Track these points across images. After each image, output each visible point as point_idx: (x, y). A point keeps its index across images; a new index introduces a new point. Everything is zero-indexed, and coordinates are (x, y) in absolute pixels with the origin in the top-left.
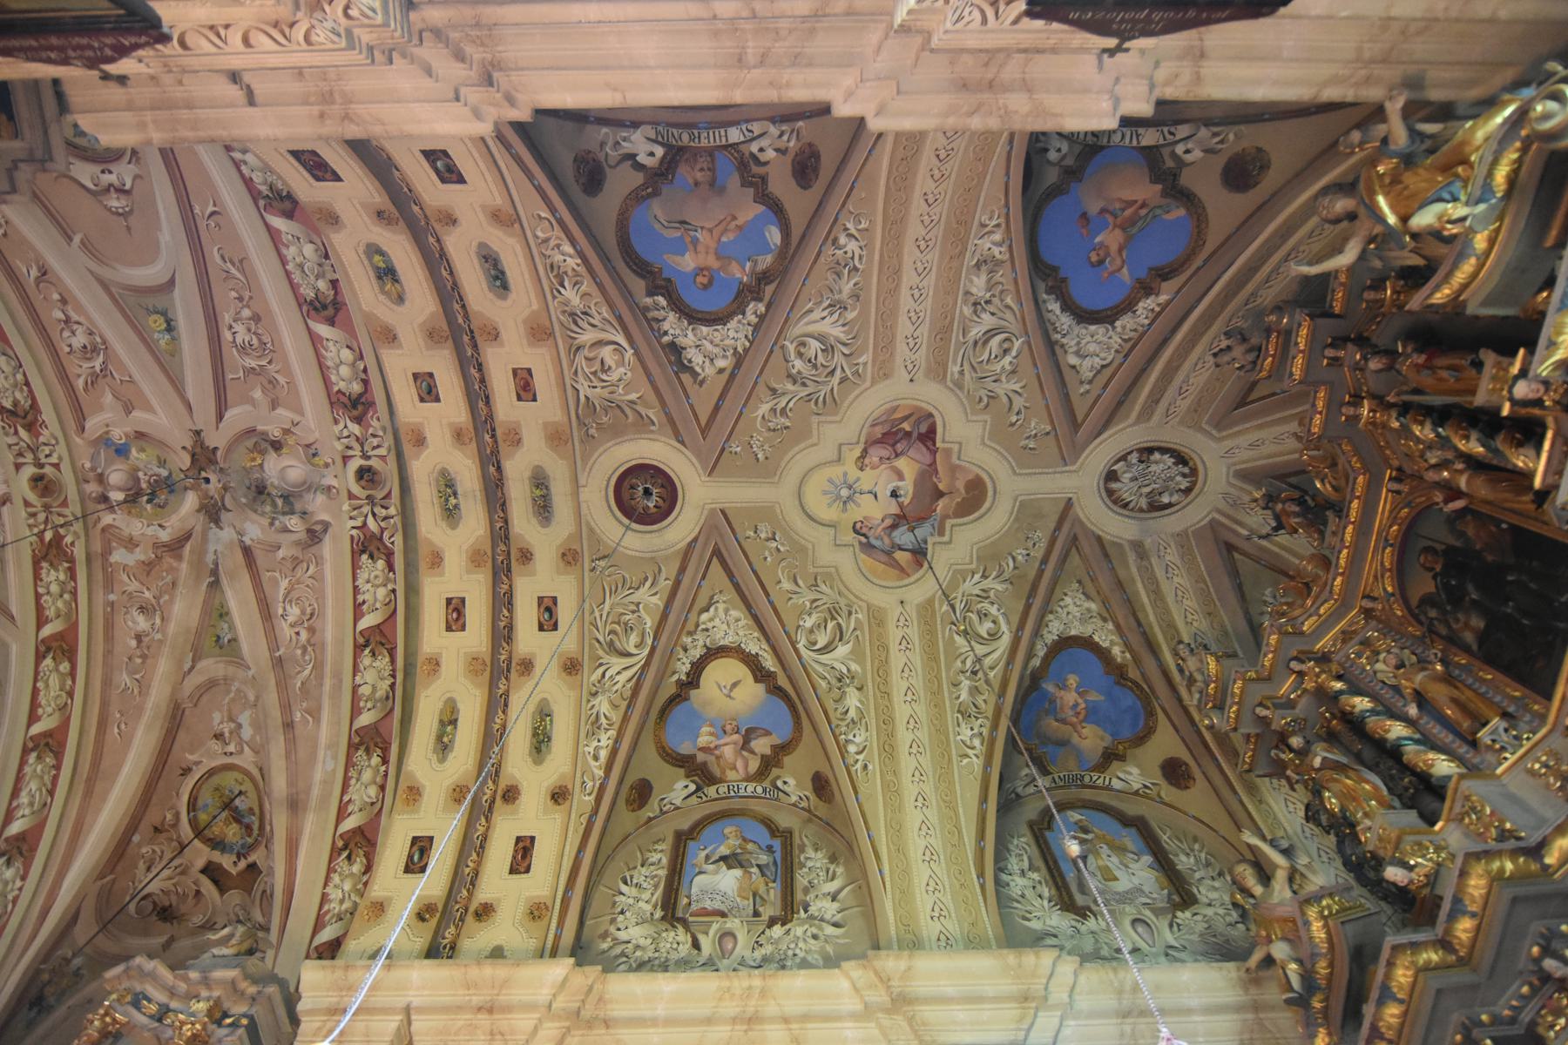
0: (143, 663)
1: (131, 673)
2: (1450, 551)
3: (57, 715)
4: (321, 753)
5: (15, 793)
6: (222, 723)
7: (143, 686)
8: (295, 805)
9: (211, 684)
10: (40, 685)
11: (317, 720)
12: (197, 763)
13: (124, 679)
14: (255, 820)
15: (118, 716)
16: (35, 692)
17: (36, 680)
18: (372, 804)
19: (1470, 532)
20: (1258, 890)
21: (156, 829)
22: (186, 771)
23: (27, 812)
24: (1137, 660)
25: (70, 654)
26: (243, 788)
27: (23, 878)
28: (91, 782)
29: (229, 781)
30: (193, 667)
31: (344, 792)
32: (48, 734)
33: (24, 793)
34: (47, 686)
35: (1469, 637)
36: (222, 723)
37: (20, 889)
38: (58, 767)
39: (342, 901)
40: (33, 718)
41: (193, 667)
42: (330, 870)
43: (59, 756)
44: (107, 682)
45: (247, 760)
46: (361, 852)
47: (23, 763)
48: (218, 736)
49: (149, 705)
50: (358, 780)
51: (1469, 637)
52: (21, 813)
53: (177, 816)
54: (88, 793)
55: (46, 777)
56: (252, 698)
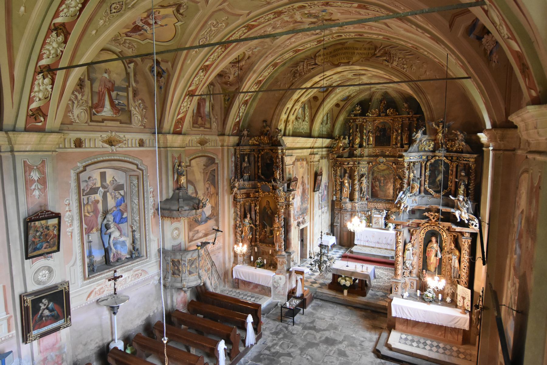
2: (385, 128)
8: (254, 72)
16: (235, 33)
20: (341, 139)
23: (211, 60)
24: (352, 98)
27: (204, 76)
38: (223, 52)
51: (377, 134)
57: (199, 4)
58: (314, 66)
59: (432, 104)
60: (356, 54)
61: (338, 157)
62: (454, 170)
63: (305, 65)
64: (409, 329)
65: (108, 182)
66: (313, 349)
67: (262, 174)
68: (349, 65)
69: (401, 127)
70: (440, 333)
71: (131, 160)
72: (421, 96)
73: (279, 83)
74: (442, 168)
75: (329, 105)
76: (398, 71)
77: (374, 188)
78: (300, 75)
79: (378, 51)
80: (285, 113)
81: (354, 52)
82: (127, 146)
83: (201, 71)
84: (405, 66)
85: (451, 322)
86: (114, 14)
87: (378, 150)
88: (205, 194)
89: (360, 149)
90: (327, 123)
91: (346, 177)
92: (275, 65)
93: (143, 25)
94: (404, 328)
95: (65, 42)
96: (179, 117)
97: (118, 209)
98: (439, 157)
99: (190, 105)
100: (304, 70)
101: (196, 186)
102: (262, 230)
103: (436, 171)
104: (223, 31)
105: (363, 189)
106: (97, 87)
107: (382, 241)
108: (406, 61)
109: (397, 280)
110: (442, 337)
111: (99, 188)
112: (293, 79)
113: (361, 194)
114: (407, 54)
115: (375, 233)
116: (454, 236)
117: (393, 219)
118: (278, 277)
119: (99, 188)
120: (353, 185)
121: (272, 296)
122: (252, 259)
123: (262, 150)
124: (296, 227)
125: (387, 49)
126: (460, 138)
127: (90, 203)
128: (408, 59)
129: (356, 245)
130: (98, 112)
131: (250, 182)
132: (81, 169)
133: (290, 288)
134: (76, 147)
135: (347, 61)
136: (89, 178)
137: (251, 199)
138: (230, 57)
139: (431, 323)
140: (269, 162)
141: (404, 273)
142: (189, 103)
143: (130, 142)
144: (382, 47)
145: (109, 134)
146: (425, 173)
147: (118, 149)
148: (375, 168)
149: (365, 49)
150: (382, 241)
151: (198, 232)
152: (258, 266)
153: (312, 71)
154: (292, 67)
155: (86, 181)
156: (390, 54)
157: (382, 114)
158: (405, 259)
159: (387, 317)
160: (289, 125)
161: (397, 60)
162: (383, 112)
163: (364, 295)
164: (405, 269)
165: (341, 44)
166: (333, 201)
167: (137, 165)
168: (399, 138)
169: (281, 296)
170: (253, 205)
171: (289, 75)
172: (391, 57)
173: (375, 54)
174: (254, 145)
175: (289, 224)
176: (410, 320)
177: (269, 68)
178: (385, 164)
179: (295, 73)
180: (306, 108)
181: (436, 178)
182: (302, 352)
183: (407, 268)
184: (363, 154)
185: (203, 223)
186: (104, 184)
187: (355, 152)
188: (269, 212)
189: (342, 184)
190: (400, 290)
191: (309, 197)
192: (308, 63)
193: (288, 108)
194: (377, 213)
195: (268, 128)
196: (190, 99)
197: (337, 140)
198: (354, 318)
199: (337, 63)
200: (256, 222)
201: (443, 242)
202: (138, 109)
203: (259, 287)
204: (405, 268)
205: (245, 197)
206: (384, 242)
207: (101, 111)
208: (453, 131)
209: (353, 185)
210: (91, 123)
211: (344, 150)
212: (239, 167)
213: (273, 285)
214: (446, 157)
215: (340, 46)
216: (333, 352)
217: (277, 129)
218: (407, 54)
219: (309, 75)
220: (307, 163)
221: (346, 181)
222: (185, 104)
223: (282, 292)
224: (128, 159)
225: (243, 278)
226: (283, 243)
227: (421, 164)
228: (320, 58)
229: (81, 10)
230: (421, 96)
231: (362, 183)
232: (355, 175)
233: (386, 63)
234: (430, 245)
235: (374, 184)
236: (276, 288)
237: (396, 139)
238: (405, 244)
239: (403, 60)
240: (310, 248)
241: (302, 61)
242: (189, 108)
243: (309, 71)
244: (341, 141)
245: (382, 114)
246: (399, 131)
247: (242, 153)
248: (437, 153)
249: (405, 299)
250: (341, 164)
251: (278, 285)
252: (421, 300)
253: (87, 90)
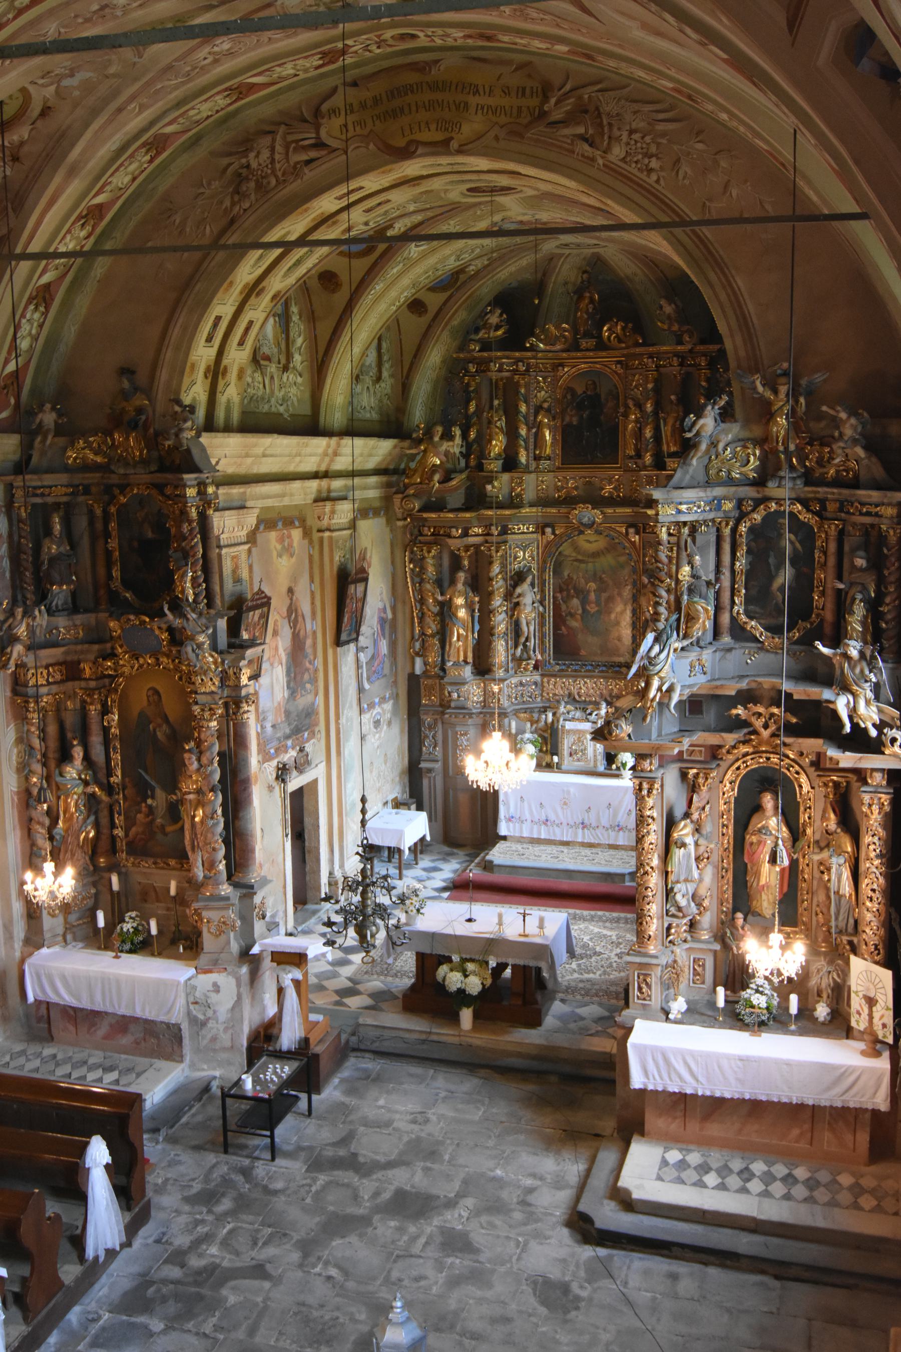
2: (598, 396)
8: (72, 172)
11: (140, 113)
19: (610, 404)
20: (436, 439)
31: (112, 175)
35: (567, 419)
51: (567, 419)
56: (112, 70)
58: (313, 154)
59: (751, 308)
60: (472, 110)
61: (424, 509)
62: (832, 547)
63: (279, 148)
64: (693, 1126)
66: (347, 1240)
67: (127, 583)
68: (449, 153)
69: (653, 389)
70: (796, 1132)
72: (712, 276)
73: (178, 219)
74: (788, 541)
75: (382, 307)
76: (627, 179)
77: (564, 622)
78: (259, 186)
79: (553, 101)
80: (209, 339)
81: (466, 104)
84: (654, 164)
85: (829, 1089)
87: (573, 481)
89: (506, 477)
90: (379, 379)
91: (460, 586)
92: (157, 145)
94: (674, 1126)
98: (779, 501)
100: (274, 172)
102: (139, 804)
103: (772, 553)
105: (525, 629)
107: (598, 820)
108: (659, 145)
109: (646, 955)
110: (803, 1145)
112: (233, 204)
113: (516, 647)
114: (661, 116)
115: (572, 790)
116: (836, 785)
117: (624, 735)
118: (205, 981)
120: (484, 615)
121: (187, 1059)
122: (101, 923)
123: (123, 488)
124: (275, 784)
125: (586, 93)
126: (848, 432)
128: (664, 134)
129: (504, 838)
131: (79, 619)
133: (257, 1021)
135: (439, 136)
137: (83, 684)
139: (764, 1098)
140: (150, 535)
141: (669, 928)
144: (568, 87)
146: (733, 564)
148: (566, 549)
149: (506, 91)
150: (598, 820)
152: (127, 946)
153: (309, 174)
154: (230, 154)
156: (599, 115)
157: (584, 344)
158: (672, 878)
159: (613, 1094)
160: (227, 385)
161: (625, 136)
162: (587, 335)
163: (535, 1021)
164: (673, 916)
165: (414, 67)
166: (413, 680)
168: (648, 433)
169: (224, 1056)
170: (94, 710)
171: (216, 184)
172: (601, 125)
173: (543, 114)
174: (87, 467)
175: (242, 776)
176: (694, 1096)
177: (132, 156)
178: (600, 533)
179: (239, 179)
180: (295, 318)
181: (771, 578)
182: (306, 1255)
183: (679, 909)
184: (519, 495)
187: (489, 487)
188: (159, 734)
189: (446, 612)
190: (656, 995)
191: (321, 668)
192: (290, 138)
193: (218, 319)
194: (578, 714)
195: (140, 401)
197: (419, 441)
198: (500, 1110)
199: (401, 143)
200: (110, 773)
201: (802, 809)
203: (132, 1027)
204: (673, 910)
205: (58, 677)
206: (604, 822)
208: (824, 408)
209: (484, 615)
211: (446, 479)
212: (27, 559)
213: (189, 1013)
214: (805, 503)
215: (412, 78)
216: (423, 1240)
217: (178, 402)
218: (661, 116)
219: (294, 187)
220: (307, 534)
221: (460, 601)
223: (225, 1039)
225: (68, 999)
226: (222, 852)
227: (718, 530)
228: (337, 122)
230: (712, 276)
231: (517, 604)
232: (492, 574)
233: (586, 147)
234: (756, 823)
235: (564, 607)
236: (199, 1024)
237: (639, 434)
238: (670, 824)
239: (648, 139)
240: (331, 861)
241: (267, 129)
243: (295, 171)
244: (435, 446)
245: (584, 344)
246: (649, 407)
247: (38, 500)
248: (772, 489)
249: (676, 1022)
250: (440, 536)
251: (210, 1013)
252: (728, 1020)
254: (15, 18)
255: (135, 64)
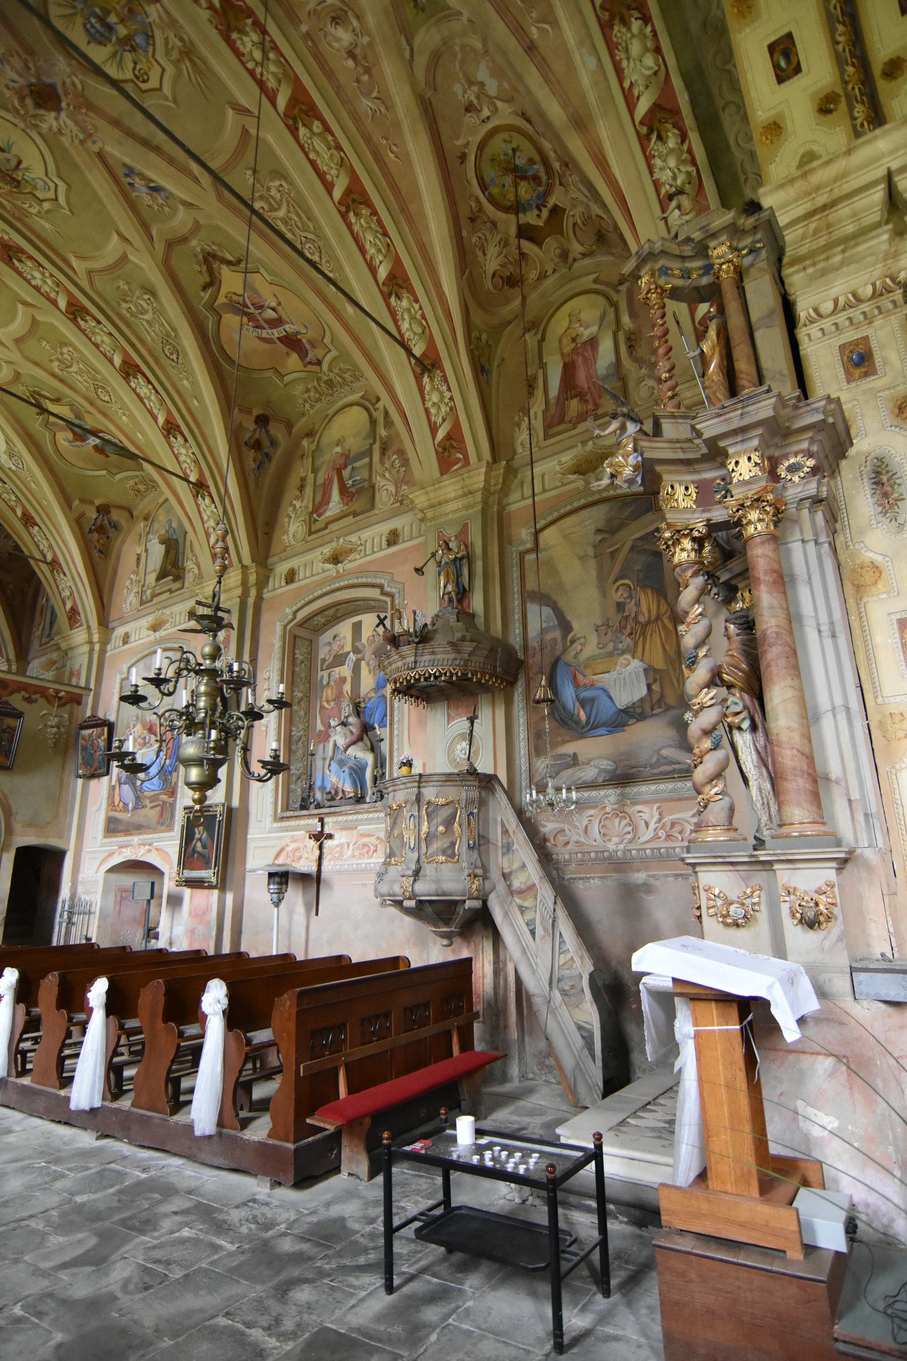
0: (370, 76)
1: (367, 95)
3: (341, 171)
4: (577, 58)
5: (363, 251)
6: (465, 92)
7: (384, 100)
9: (436, 58)
10: (312, 156)
12: (467, 145)
13: (366, 104)
14: (539, 169)
15: (384, 142)
16: (313, 163)
17: (306, 155)
18: (656, 73)
21: (472, 220)
22: (463, 157)
23: (381, 258)
25: (312, 112)
26: (514, 145)
27: (417, 301)
28: (404, 209)
29: (499, 145)
30: (412, 51)
31: (621, 80)
32: (348, 192)
33: (368, 247)
34: (317, 152)
36: (465, 92)
37: (421, 308)
38: (374, 213)
39: (674, 178)
40: (329, 187)
41: (412, 51)
42: (648, 159)
43: (368, 203)
44: (355, 117)
45: (505, 114)
46: (669, 126)
47: (349, 226)
48: (469, 108)
49: (401, 114)
50: (628, 59)
52: (378, 262)
53: (477, 200)
54: (410, 219)
55: (373, 226)
57: (202, 222)
65: (364, 640)
71: (369, 580)
82: (363, 554)
83: (393, 300)
86: (180, 361)
88: (607, 624)
93: (281, 329)
95: (186, 440)
96: (441, 435)
97: (380, 694)
99: (449, 390)
101: (561, 604)
104: (299, 192)
106: (321, 477)
111: (348, 653)
119: (348, 653)
127: (332, 683)
130: (319, 516)
132: (291, 617)
134: (287, 583)
136: (335, 637)
138: (426, 197)
142: (445, 388)
143: (369, 545)
145: (334, 545)
147: (347, 567)
151: (574, 761)
155: (330, 644)
167: (381, 587)
185: (601, 731)
186: (357, 644)
196: (437, 380)
202: (390, 473)
207: (325, 511)
210: (309, 538)
222: (435, 398)
224: (364, 580)
229: (157, 392)
242: (451, 399)
253: (309, 490)
254: (332, 134)
255: (470, 21)
